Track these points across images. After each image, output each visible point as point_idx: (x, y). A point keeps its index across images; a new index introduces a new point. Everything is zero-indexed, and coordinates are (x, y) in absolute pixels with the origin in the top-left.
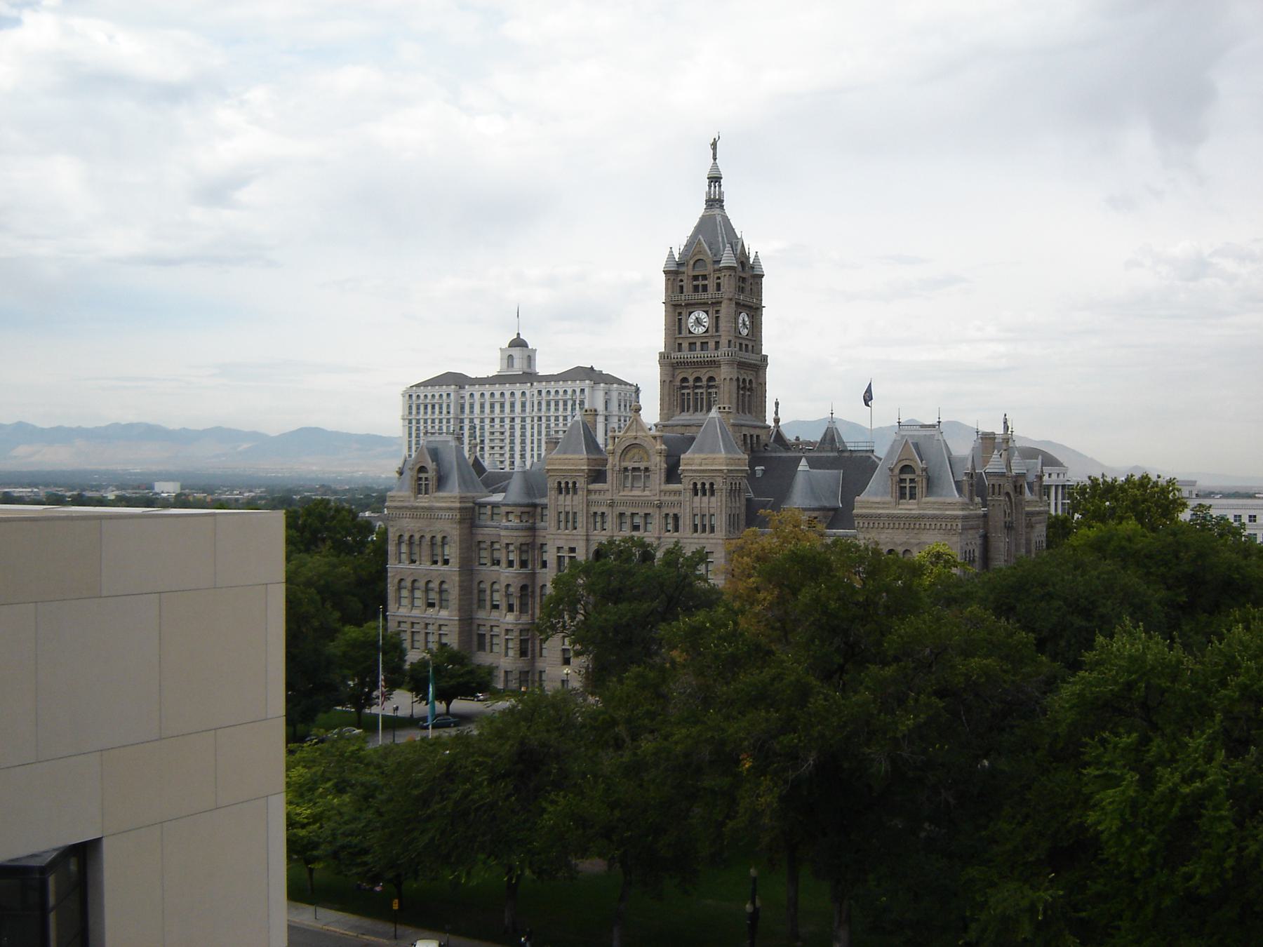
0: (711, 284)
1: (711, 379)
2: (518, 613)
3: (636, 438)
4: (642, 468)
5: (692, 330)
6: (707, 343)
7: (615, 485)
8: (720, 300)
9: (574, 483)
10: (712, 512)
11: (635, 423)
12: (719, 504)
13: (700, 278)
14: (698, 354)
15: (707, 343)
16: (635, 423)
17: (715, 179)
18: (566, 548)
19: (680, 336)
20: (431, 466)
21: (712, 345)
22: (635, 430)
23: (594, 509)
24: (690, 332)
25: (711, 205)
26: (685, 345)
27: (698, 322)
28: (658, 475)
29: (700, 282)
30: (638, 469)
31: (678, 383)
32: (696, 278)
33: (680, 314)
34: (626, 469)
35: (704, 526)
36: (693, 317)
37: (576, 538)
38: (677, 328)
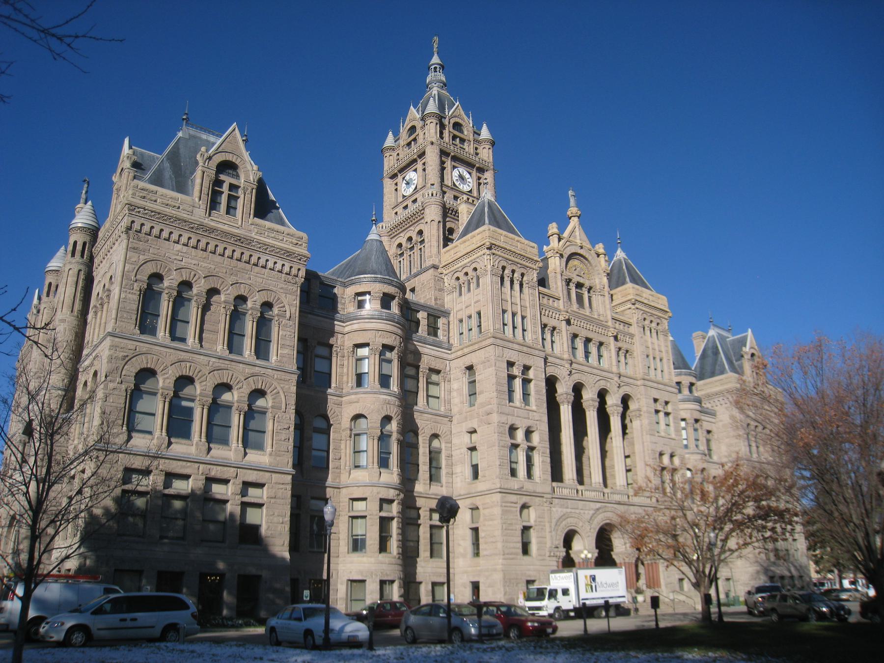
5: (457, 184)
13: (458, 140)
24: (454, 185)
36: (456, 173)
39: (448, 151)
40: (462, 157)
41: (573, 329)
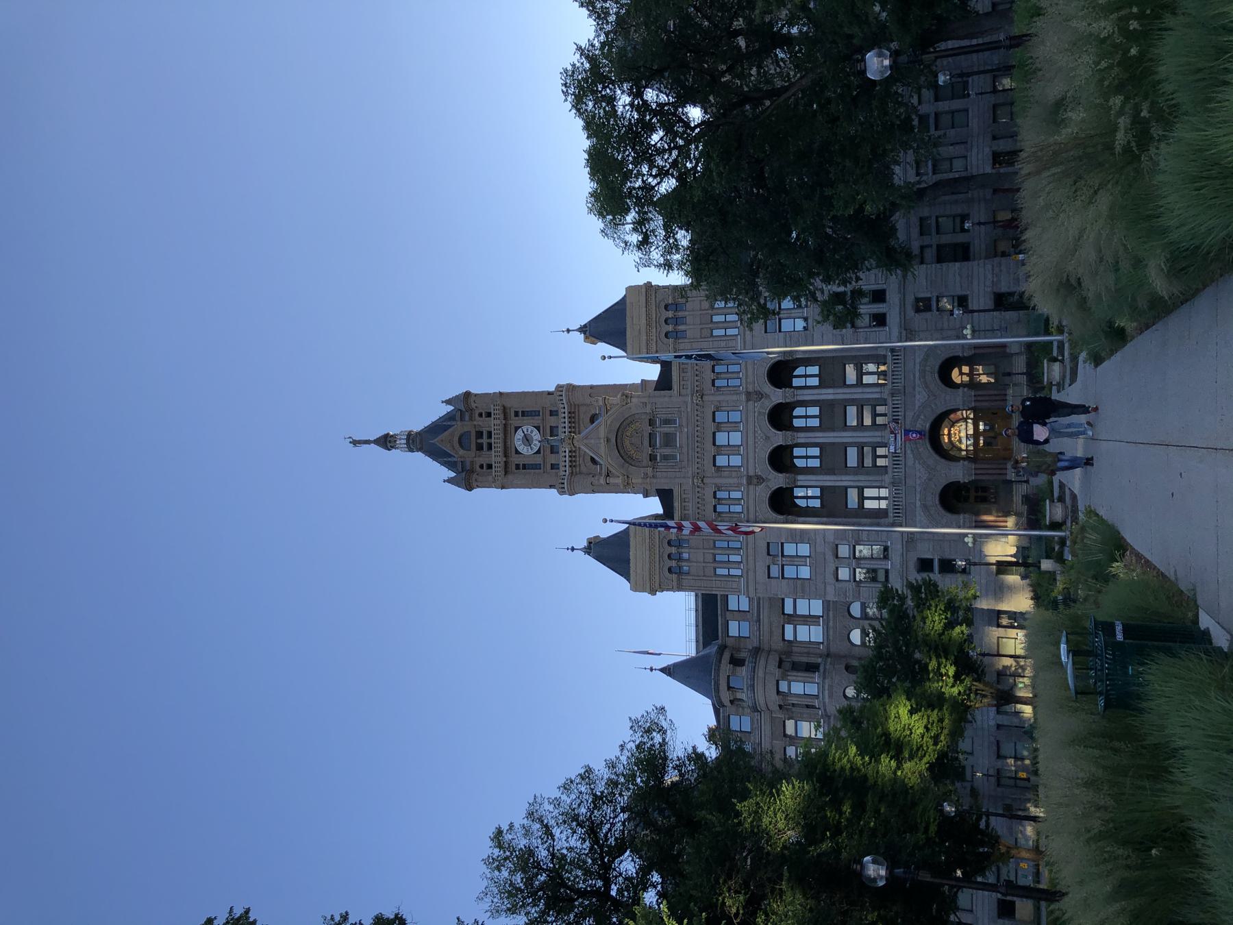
3: (608, 440)
5: (536, 449)
13: (479, 441)
17: (386, 442)
21: (552, 421)
24: (538, 452)
26: (552, 459)
29: (484, 441)
32: (480, 447)
33: (517, 467)
34: (652, 458)
36: (522, 449)
39: (502, 463)
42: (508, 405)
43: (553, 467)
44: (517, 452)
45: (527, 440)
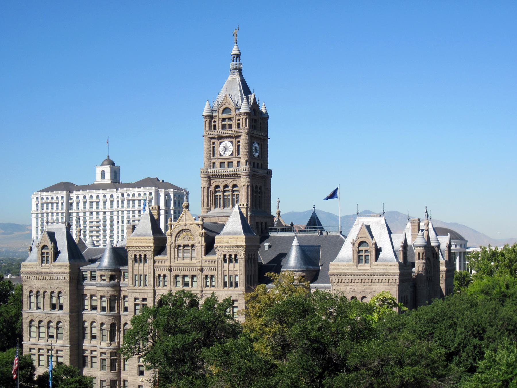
0: (234, 123)
1: (235, 186)
2: (109, 341)
4: (190, 245)
5: (222, 154)
6: (232, 162)
7: (172, 257)
8: (240, 134)
9: (145, 256)
10: (236, 273)
11: (185, 214)
12: (241, 268)
13: (227, 119)
14: (226, 170)
15: (232, 162)
16: (185, 215)
18: (140, 298)
19: (214, 158)
20: (50, 245)
21: (235, 163)
22: (185, 220)
23: (157, 273)
24: (221, 155)
25: (234, 72)
26: (217, 164)
27: (226, 149)
28: (200, 250)
29: (227, 123)
30: (188, 246)
31: (212, 188)
32: (224, 120)
33: (214, 143)
34: (179, 246)
35: (231, 283)
37: (147, 291)
38: (212, 152)
40: (223, 135)
41: (174, 273)
42: (242, 137)
43: (214, 163)
44: (221, 143)
45: (226, 149)
